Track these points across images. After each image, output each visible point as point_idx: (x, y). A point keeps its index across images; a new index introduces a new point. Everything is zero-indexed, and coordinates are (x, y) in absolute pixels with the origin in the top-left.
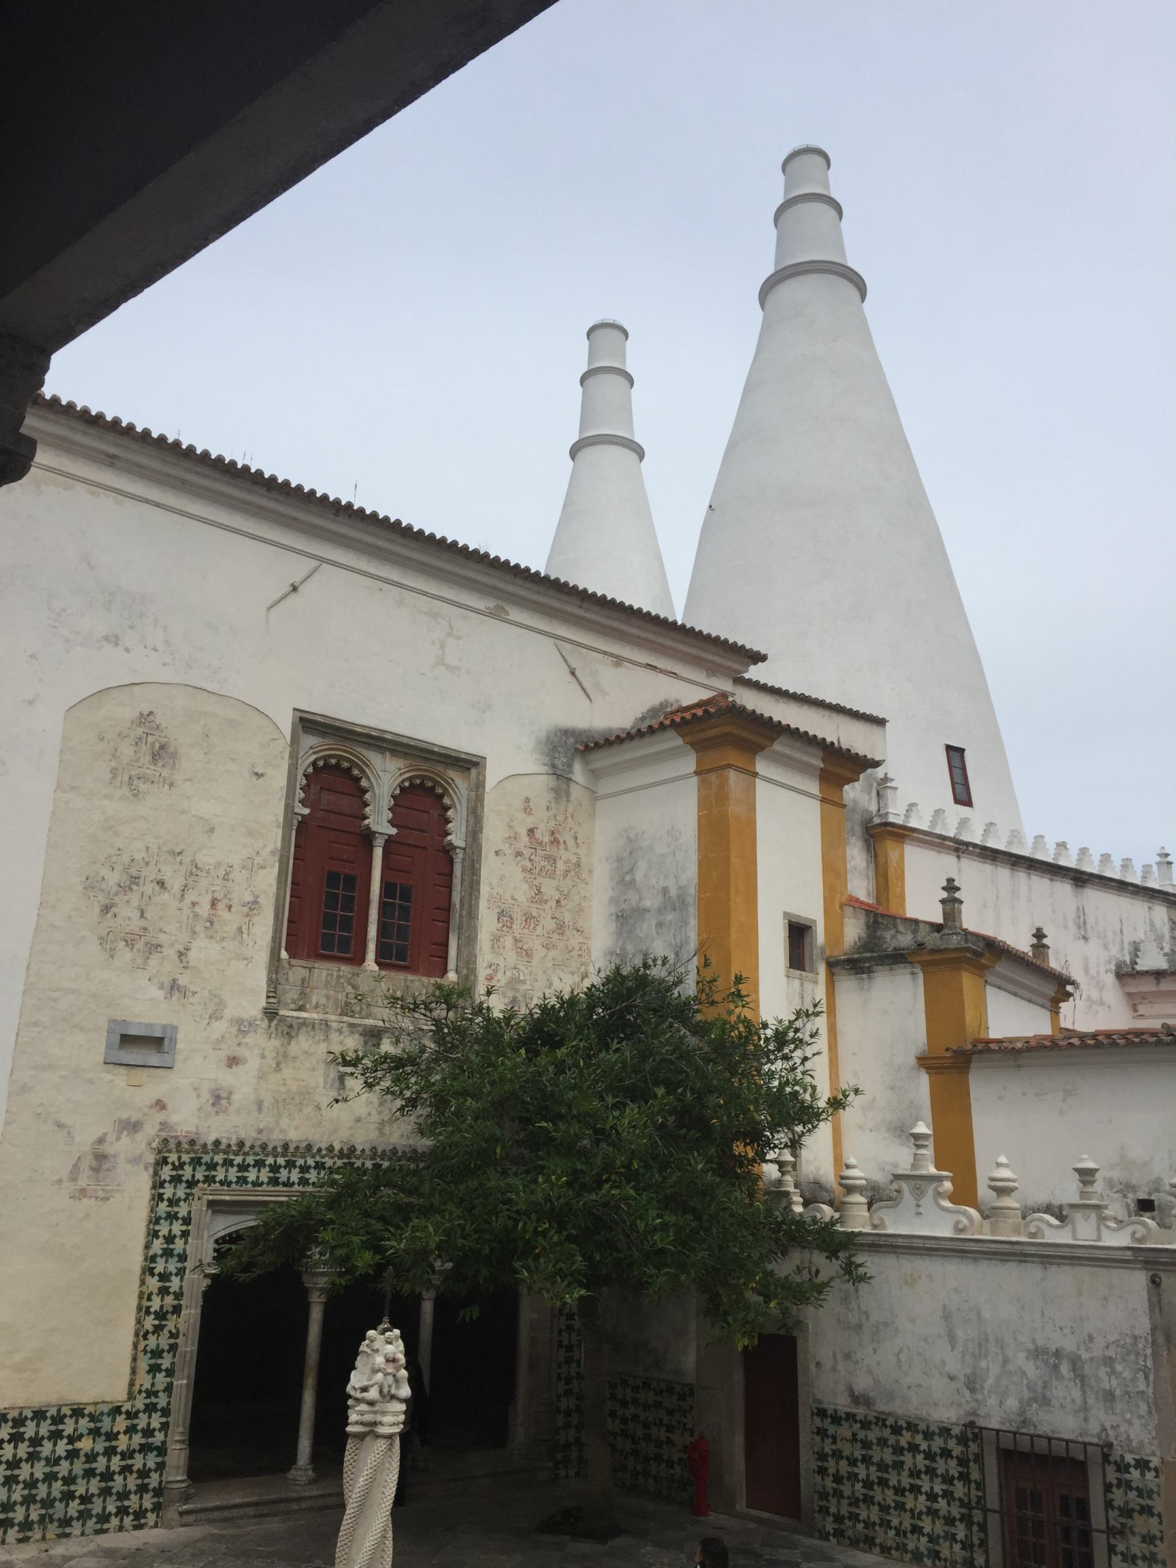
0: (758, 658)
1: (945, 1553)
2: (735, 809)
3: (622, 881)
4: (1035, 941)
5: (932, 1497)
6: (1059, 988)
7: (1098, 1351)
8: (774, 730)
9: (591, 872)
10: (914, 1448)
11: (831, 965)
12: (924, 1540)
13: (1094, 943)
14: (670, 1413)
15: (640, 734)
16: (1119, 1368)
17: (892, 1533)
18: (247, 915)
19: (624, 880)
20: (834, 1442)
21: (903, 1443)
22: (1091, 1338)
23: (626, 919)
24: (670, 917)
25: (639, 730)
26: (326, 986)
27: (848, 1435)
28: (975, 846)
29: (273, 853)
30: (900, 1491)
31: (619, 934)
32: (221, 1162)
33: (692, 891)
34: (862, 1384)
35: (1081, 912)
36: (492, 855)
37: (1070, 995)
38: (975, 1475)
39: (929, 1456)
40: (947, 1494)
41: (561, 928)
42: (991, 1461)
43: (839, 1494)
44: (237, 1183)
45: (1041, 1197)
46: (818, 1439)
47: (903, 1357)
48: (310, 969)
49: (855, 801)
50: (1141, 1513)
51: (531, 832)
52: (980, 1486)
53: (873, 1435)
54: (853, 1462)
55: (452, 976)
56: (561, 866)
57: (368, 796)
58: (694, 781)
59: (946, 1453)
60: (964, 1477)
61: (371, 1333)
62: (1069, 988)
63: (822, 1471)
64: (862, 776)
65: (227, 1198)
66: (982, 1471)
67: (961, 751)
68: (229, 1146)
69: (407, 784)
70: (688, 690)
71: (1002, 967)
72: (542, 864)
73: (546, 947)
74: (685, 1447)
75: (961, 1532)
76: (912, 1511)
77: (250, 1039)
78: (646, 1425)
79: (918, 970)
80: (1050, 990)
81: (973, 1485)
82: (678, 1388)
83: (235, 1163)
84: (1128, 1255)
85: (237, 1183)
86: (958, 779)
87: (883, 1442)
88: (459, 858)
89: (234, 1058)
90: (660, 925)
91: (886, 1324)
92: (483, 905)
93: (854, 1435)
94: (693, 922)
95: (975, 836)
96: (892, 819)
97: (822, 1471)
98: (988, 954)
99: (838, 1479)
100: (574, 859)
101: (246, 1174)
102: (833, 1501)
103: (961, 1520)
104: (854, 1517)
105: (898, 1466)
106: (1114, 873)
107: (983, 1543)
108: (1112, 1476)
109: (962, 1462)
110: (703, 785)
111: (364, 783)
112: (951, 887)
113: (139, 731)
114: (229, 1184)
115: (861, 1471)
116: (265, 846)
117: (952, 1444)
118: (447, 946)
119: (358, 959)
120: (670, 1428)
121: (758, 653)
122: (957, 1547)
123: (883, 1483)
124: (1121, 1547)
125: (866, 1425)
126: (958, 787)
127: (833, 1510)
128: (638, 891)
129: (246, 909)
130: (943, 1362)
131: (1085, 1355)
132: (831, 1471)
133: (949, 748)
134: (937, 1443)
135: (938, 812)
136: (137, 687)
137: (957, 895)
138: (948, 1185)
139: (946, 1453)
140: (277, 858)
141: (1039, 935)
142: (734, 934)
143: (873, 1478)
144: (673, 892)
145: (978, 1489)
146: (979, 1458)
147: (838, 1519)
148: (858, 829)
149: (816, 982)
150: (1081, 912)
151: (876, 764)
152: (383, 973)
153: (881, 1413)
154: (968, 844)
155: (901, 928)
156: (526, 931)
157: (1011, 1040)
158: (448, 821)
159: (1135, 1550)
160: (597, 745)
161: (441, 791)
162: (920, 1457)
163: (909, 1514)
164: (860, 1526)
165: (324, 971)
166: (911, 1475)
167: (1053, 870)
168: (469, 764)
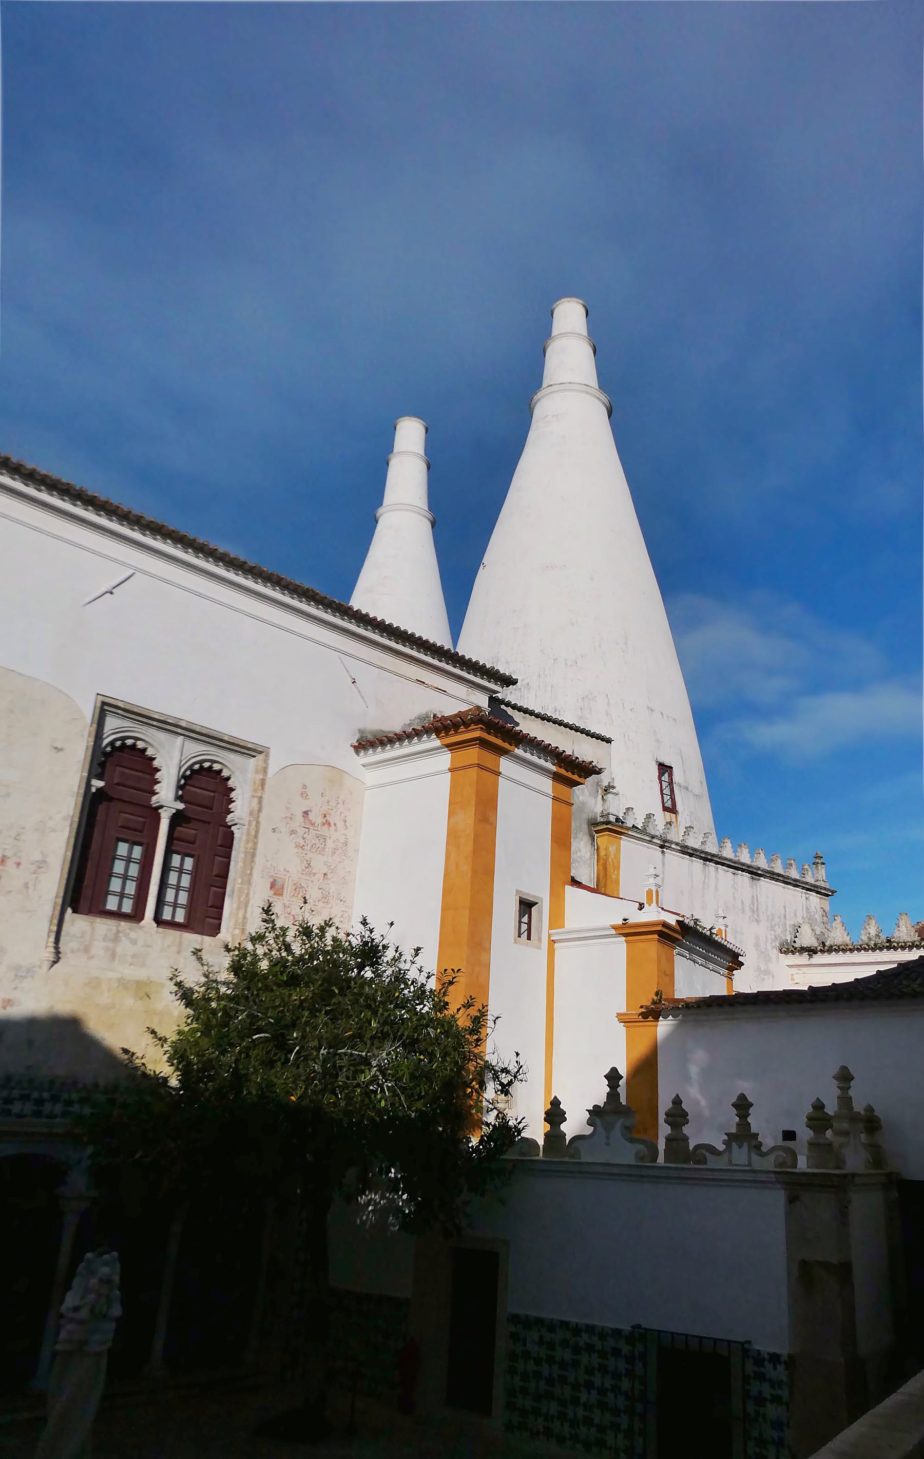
0: (508, 681)
9: (357, 851)
20: (524, 1343)
26: (105, 939)
29: (64, 818)
35: (754, 899)
49: (583, 803)
50: (772, 1401)
51: (306, 813)
54: (538, 1362)
56: (330, 844)
57: (158, 775)
72: (313, 842)
75: (624, 1421)
86: (667, 791)
87: (565, 1343)
88: (239, 833)
93: (541, 1338)
95: (676, 835)
100: (342, 839)
105: (575, 1364)
115: (545, 1369)
118: (222, 908)
121: (510, 678)
124: (755, 1433)
126: (666, 798)
129: (34, 867)
135: (649, 816)
140: (69, 822)
148: (585, 826)
151: (599, 772)
152: (161, 930)
158: (231, 801)
165: (104, 926)
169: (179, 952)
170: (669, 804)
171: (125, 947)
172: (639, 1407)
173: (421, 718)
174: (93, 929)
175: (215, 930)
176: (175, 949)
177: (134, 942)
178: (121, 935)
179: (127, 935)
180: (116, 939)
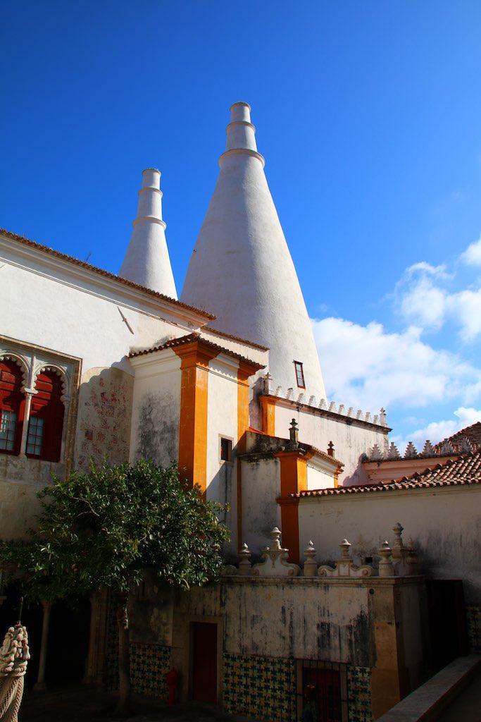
1: (279, 715)
2: (199, 386)
3: (145, 419)
4: (329, 447)
5: (274, 690)
6: (339, 467)
7: (347, 622)
8: (217, 350)
9: (131, 414)
10: (267, 669)
11: (240, 459)
12: (270, 709)
13: (353, 449)
14: (160, 659)
15: (155, 350)
16: (354, 630)
17: (256, 707)
19: (146, 419)
20: (232, 669)
21: (262, 667)
22: (344, 618)
23: (147, 438)
24: (167, 435)
25: (155, 348)
27: (239, 665)
28: (306, 406)
30: (260, 689)
31: (142, 443)
33: (178, 423)
34: (247, 642)
35: (349, 435)
36: (84, 404)
37: (342, 471)
38: (292, 680)
39: (274, 672)
40: (281, 689)
41: (115, 440)
42: (299, 673)
43: (234, 691)
45: (327, 558)
46: (225, 668)
47: (264, 630)
51: (103, 394)
52: (295, 684)
53: (249, 665)
54: (240, 677)
55: (62, 461)
56: (116, 411)
57: (24, 376)
58: (180, 372)
59: (281, 671)
60: (288, 681)
61: (12, 629)
62: (342, 468)
63: (227, 681)
64: (256, 373)
66: (296, 677)
67: (301, 364)
69: (44, 370)
70: (179, 332)
71: (314, 459)
73: (110, 449)
74: (166, 674)
75: (286, 705)
76: (265, 697)
78: (149, 665)
79: (278, 460)
80: (334, 469)
81: (292, 684)
82: (163, 648)
84: (361, 581)
86: (299, 374)
90: (162, 439)
91: (257, 616)
92: (78, 428)
93: (241, 665)
94: (177, 438)
95: (306, 401)
96: (270, 393)
97: (227, 681)
98: (308, 452)
99: (233, 685)
102: (231, 694)
103: (286, 700)
104: (240, 701)
105: (260, 677)
106: (362, 418)
107: (295, 709)
108: (350, 677)
109: (288, 674)
110: (184, 374)
111: (22, 369)
112: (293, 423)
117: (283, 666)
119: (16, 452)
120: (160, 666)
122: (284, 712)
123: (253, 685)
125: (246, 661)
127: (231, 698)
128: (152, 423)
130: (281, 632)
131: (341, 626)
132: (231, 681)
133: (296, 363)
134: (278, 666)
137: (296, 427)
138: (287, 555)
139: (281, 671)
141: (331, 445)
142: (195, 444)
143: (249, 683)
144: (169, 423)
145: (294, 686)
146: (295, 672)
147: (233, 702)
149: (233, 467)
150: (349, 435)
153: (253, 655)
154: (302, 405)
155: (271, 441)
156: (99, 441)
157: (317, 491)
158: (62, 389)
159: (359, 708)
160: (136, 355)
161: (60, 374)
162: (269, 673)
163: (264, 699)
164: (242, 705)
166: (265, 681)
167: (338, 417)
168: (75, 364)
169: (39, 471)
170: (301, 384)
171: (11, 469)
172: (293, 698)
173: (163, 340)
175: (57, 460)
176: (36, 469)
177: (15, 466)
179: (12, 463)
180: (6, 465)
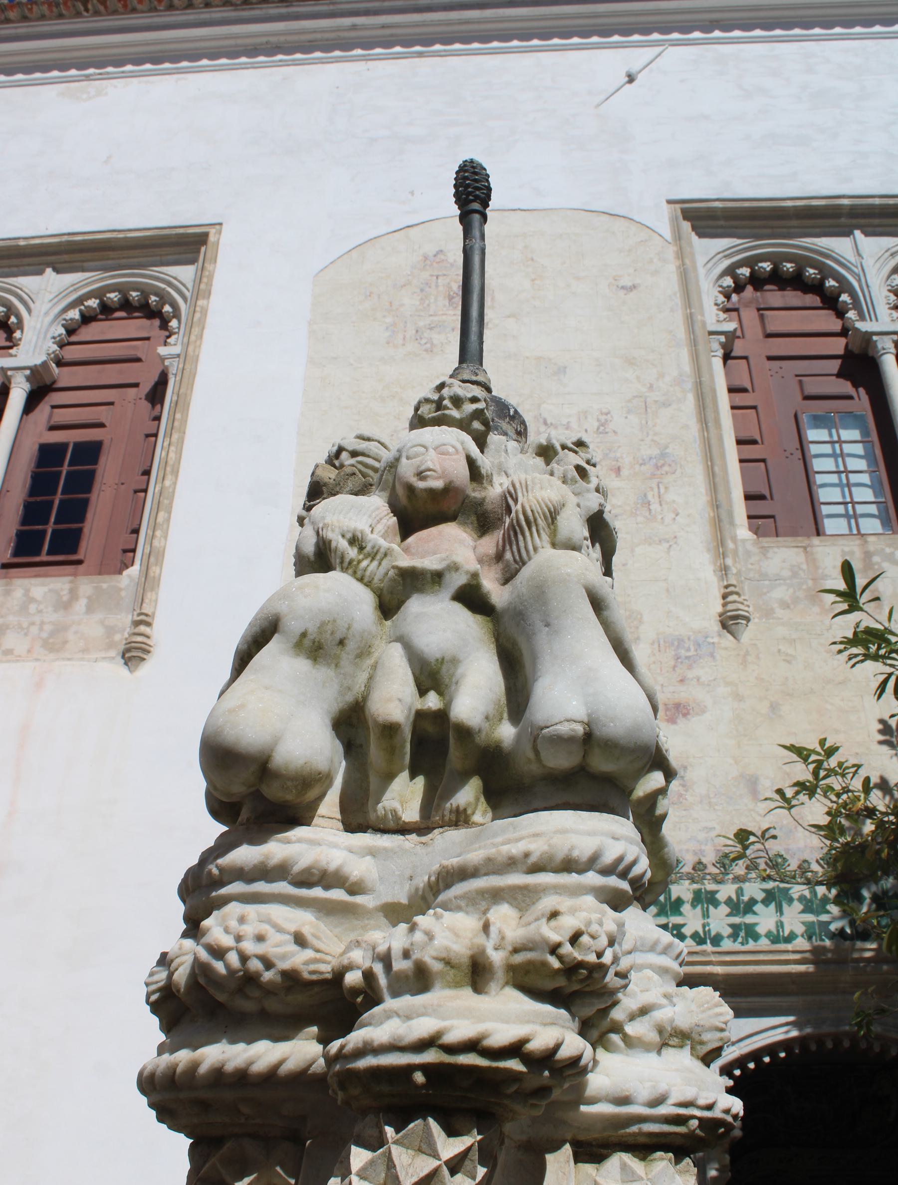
18: (653, 476)
32: (688, 896)
44: (734, 936)
48: (805, 548)
65: (719, 970)
68: (699, 866)
77: (704, 671)
83: (721, 896)
85: (734, 936)
89: (677, 706)
101: (749, 919)
113: (425, 275)
114: (716, 940)
116: (661, 375)
136: (410, 230)
140: (689, 385)
174: (812, 560)
178: (876, 559)
